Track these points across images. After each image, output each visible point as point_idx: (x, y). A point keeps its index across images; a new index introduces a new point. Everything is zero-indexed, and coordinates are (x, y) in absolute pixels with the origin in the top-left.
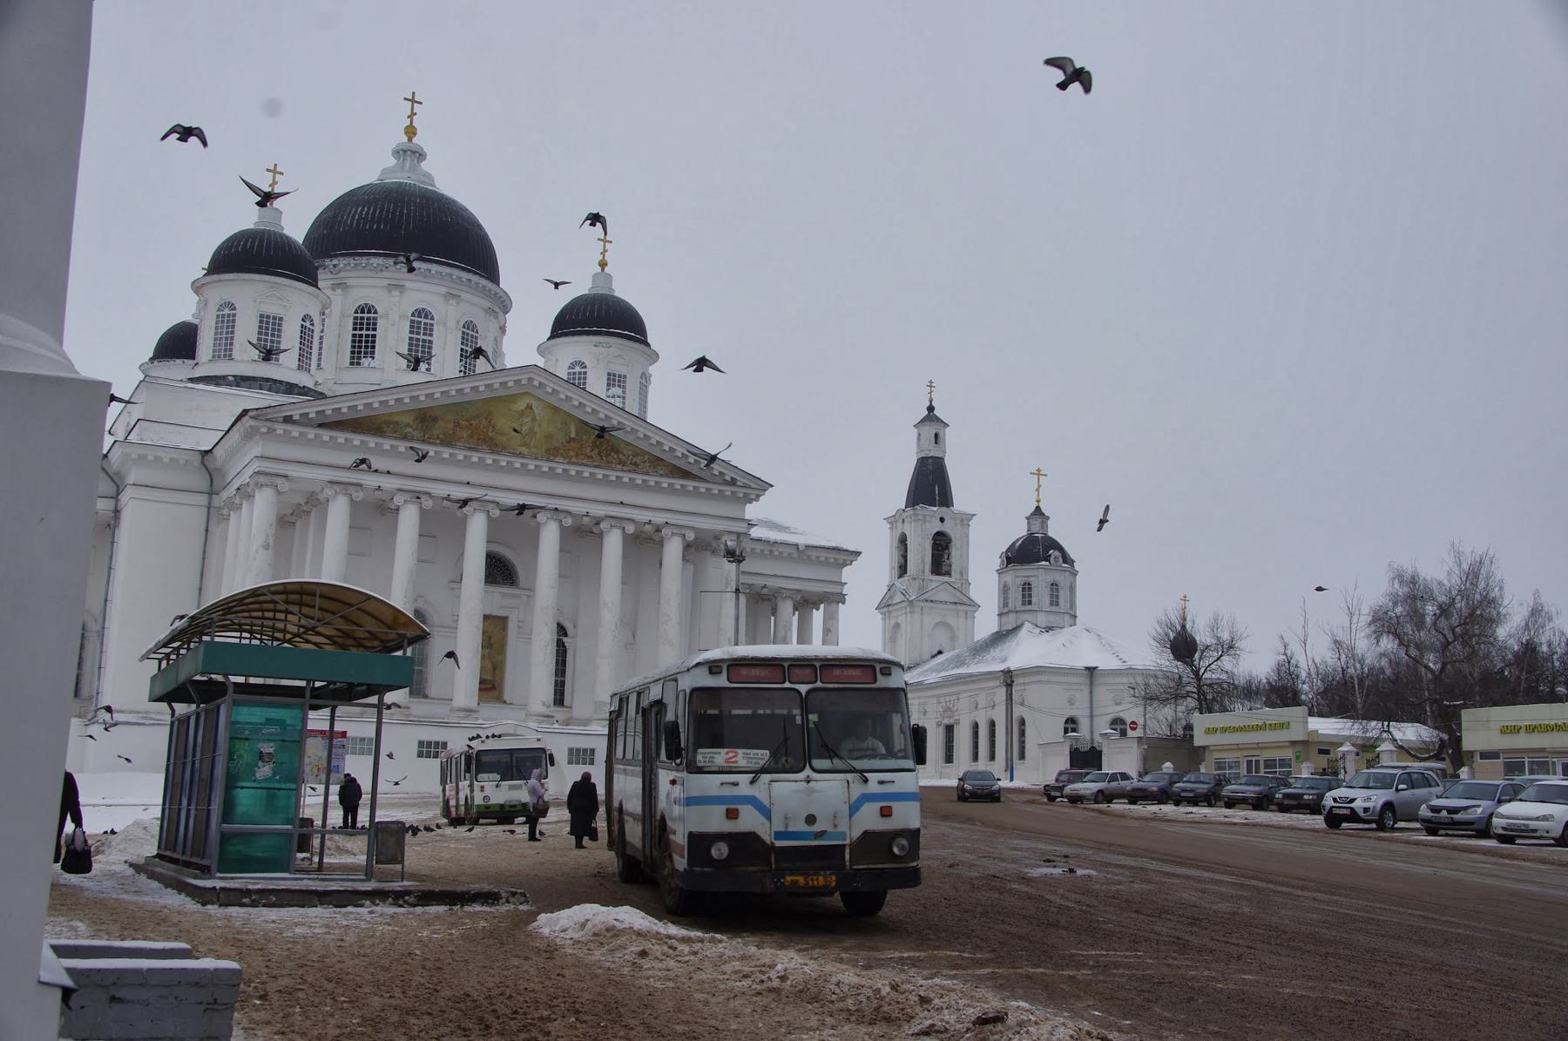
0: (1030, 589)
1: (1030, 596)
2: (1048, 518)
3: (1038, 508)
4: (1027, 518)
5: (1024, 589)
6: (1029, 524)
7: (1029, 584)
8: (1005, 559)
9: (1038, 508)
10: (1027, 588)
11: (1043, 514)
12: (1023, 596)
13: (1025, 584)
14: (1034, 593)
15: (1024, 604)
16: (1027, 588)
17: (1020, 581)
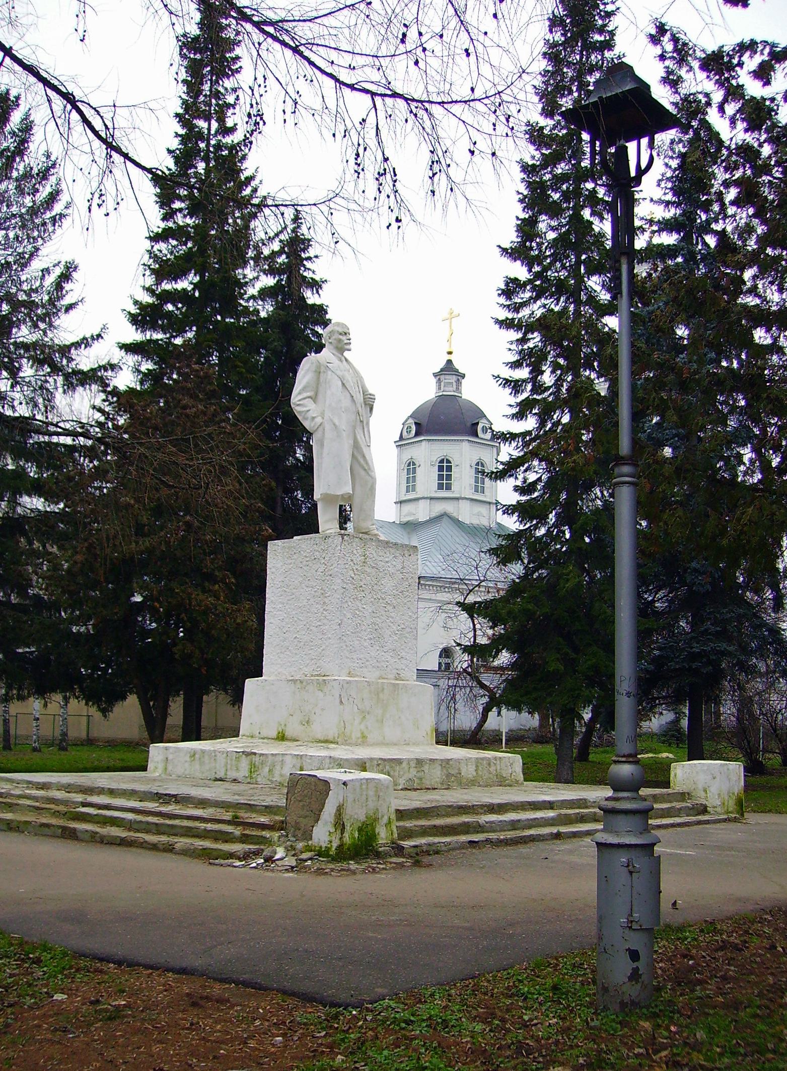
0: (449, 469)
1: (449, 477)
2: (463, 376)
3: (449, 362)
4: (435, 375)
5: (441, 469)
6: (439, 381)
7: (448, 461)
8: (414, 427)
9: (449, 362)
10: (445, 468)
11: (457, 371)
12: (441, 477)
13: (442, 461)
14: (455, 473)
15: (440, 487)
16: (445, 468)
17: (437, 455)
